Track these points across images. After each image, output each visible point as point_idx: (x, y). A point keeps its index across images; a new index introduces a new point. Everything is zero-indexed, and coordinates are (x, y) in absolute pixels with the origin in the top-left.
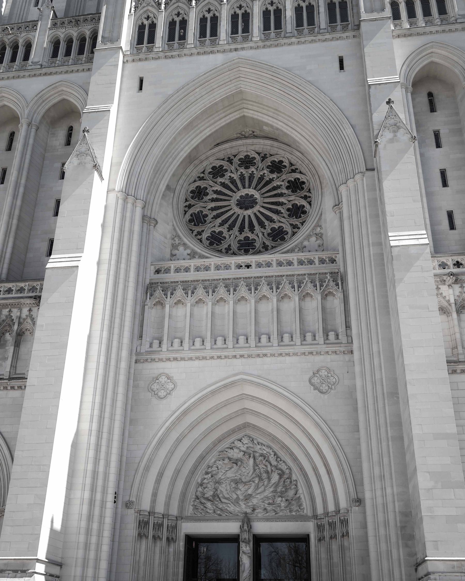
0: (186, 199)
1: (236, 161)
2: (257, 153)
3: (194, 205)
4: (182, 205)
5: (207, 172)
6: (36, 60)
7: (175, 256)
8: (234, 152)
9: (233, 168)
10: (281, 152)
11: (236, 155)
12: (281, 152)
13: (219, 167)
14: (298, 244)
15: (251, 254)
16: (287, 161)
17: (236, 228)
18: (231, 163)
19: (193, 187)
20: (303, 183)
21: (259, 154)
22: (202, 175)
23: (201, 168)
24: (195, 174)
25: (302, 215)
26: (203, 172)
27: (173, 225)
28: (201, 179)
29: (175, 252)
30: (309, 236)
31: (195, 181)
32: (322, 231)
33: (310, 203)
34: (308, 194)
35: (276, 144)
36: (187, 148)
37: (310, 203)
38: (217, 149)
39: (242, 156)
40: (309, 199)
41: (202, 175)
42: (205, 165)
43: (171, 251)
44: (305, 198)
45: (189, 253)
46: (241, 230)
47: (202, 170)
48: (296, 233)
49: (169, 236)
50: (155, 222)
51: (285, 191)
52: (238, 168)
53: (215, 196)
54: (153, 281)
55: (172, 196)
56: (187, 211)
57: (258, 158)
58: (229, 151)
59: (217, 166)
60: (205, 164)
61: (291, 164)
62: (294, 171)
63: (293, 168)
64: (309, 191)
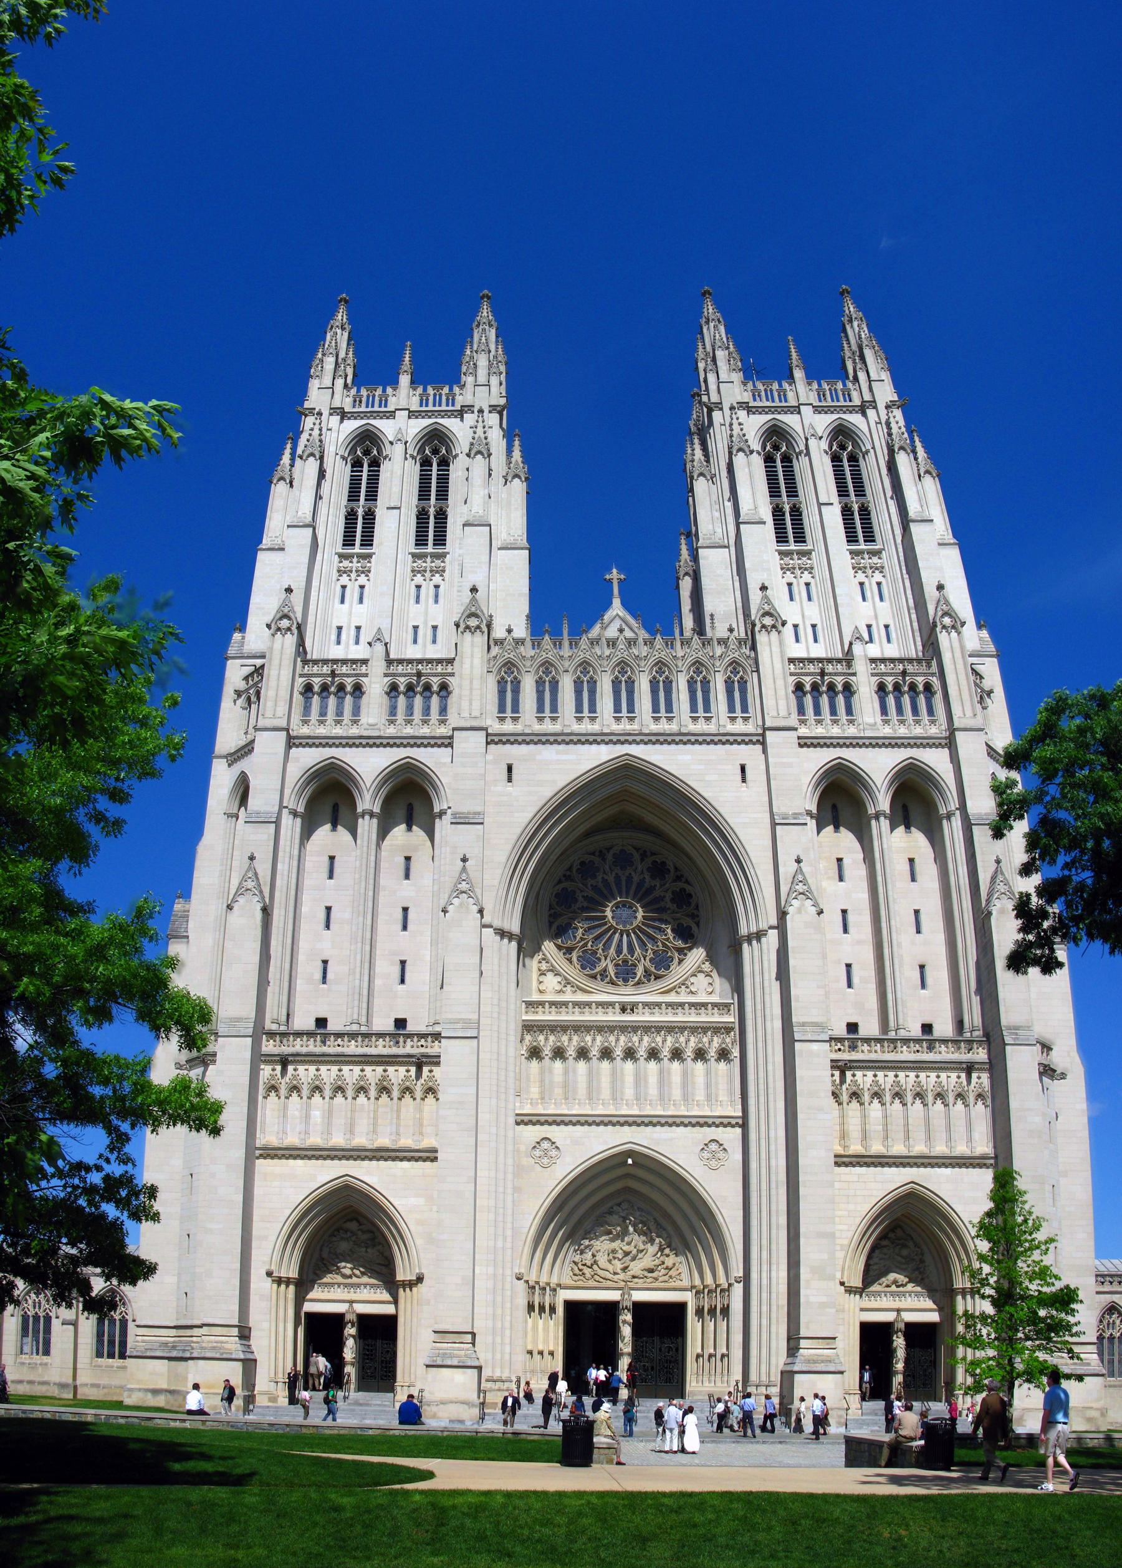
1: (610, 857)
5: (574, 870)
6: (371, 721)
9: (607, 867)
14: (686, 980)
17: (612, 950)
18: (604, 860)
20: (690, 896)
21: (637, 849)
22: (568, 873)
26: (570, 869)
28: (568, 878)
31: (560, 882)
33: (698, 924)
34: (695, 912)
37: (698, 924)
40: (696, 919)
44: (693, 916)
46: (619, 951)
51: (669, 905)
53: (585, 904)
61: (676, 869)
62: (678, 878)
63: (678, 873)
64: (697, 907)
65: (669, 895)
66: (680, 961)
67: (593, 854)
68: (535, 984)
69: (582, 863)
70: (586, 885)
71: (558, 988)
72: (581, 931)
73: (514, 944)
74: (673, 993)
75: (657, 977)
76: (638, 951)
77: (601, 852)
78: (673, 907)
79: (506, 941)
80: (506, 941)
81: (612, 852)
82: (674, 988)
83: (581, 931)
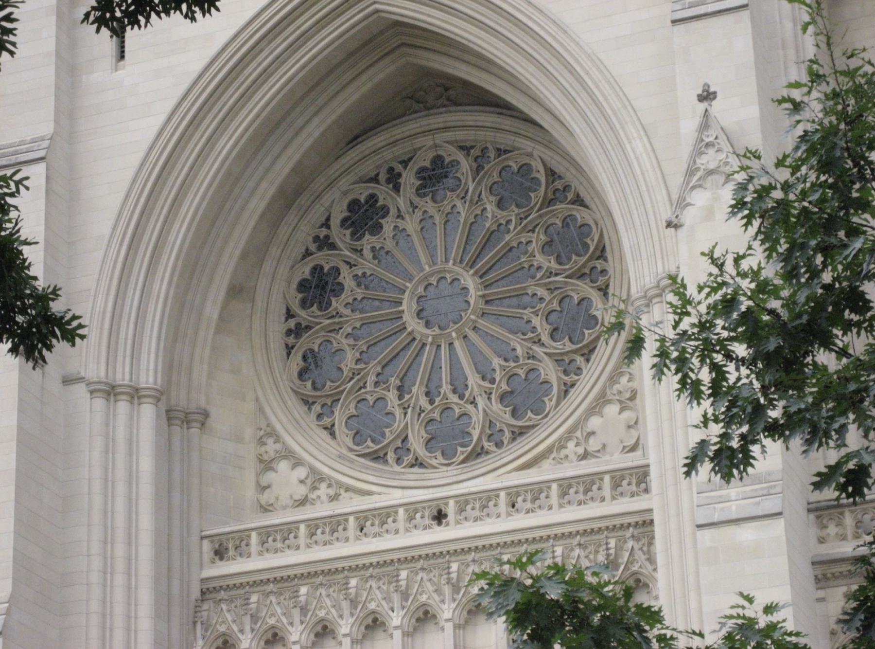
0: (288, 310)
2: (462, 148)
3: (308, 328)
4: (278, 328)
5: (335, 222)
7: (268, 491)
8: (401, 151)
9: (402, 202)
10: (521, 142)
11: (410, 159)
12: (521, 142)
13: (367, 202)
15: (463, 462)
16: (541, 168)
19: (305, 271)
22: (324, 232)
23: (317, 214)
24: (304, 235)
25: (586, 332)
27: (257, 400)
29: (270, 477)
30: (602, 400)
31: (307, 253)
32: (634, 385)
35: (507, 123)
36: (264, 185)
38: (353, 155)
39: (424, 160)
41: (324, 232)
42: (327, 204)
43: (258, 475)
45: (303, 477)
47: (323, 219)
48: (573, 385)
49: (249, 433)
50: (199, 417)
52: (416, 200)
53: (360, 293)
54: (211, 585)
55: (249, 312)
56: (293, 347)
57: (465, 165)
58: (387, 155)
59: (362, 199)
60: (326, 200)
65: (538, 238)
66: (566, 389)
67: (375, 179)
68: (250, 493)
69: (354, 205)
70: (359, 252)
71: (301, 491)
72: (350, 356)
73: (148, 412)
74: (547, 464)
75: (518, 433)
76: (473, 380)
77: (391, 170)
78: (548, 262)
79: (123, 407)
80: (123, 407)
81: (414, 167)
82: (549, 450)
83: (350, 356)
